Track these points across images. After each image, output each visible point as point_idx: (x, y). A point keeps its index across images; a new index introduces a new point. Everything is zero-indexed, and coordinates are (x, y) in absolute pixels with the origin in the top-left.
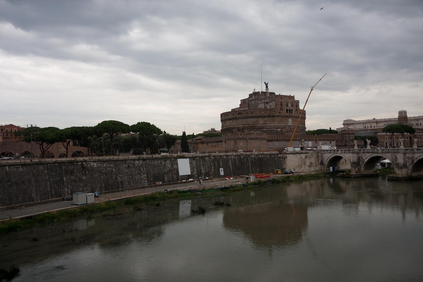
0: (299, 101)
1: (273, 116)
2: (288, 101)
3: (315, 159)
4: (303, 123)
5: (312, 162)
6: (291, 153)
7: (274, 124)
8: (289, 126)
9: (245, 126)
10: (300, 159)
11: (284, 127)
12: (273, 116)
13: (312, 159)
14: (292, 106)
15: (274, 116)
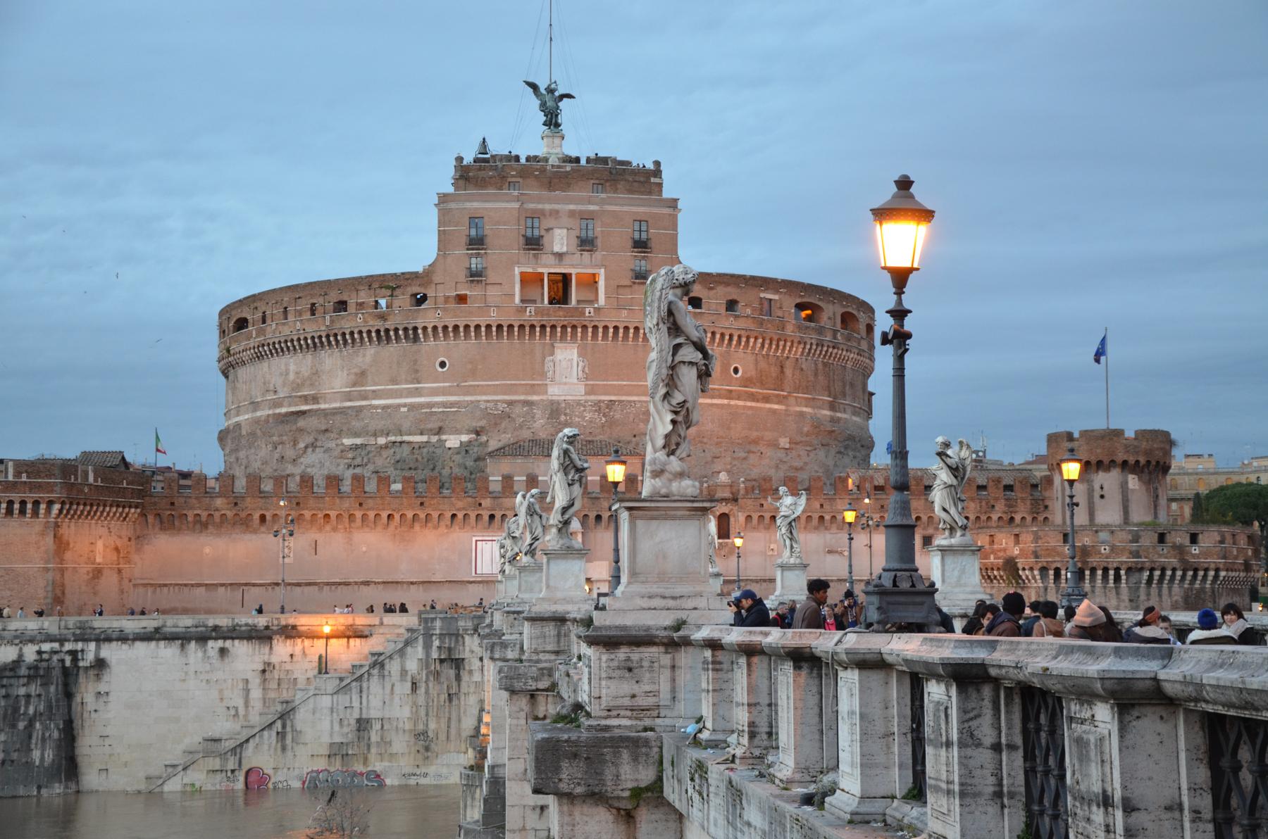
0: (676, 200)
1: (412, 334)
2: (547, 207)
3: (414, 686)
4: (747, 382)
5: (374, 714)
6: (157, 630)
7: (418, 393)
8: (555, 411)
9: (259, 414)
10: (255, 681)
11: (499, 419)
12: (412, 334)
13: (374, 685)
14: (586, 244)
15: (415, 329)
